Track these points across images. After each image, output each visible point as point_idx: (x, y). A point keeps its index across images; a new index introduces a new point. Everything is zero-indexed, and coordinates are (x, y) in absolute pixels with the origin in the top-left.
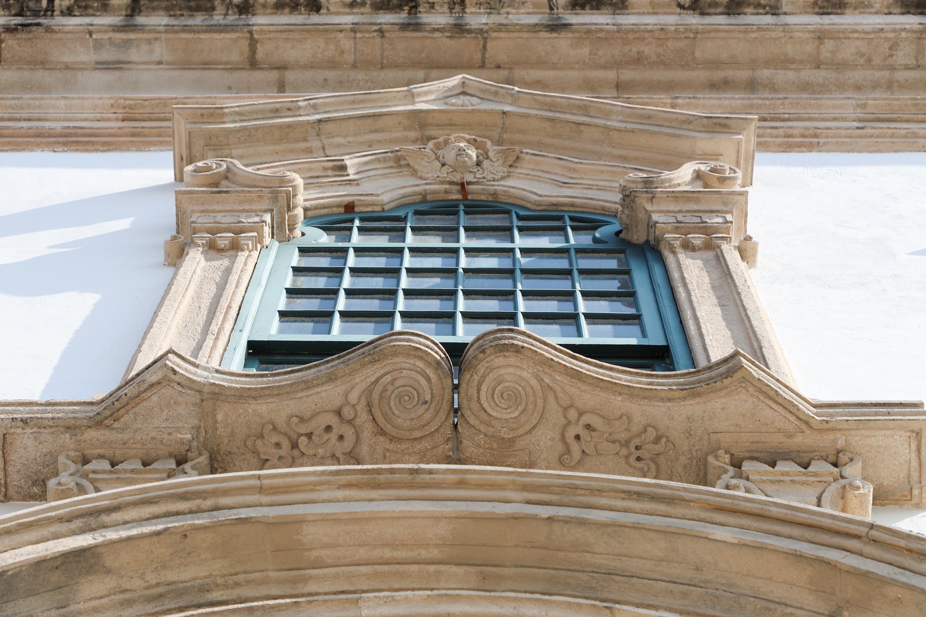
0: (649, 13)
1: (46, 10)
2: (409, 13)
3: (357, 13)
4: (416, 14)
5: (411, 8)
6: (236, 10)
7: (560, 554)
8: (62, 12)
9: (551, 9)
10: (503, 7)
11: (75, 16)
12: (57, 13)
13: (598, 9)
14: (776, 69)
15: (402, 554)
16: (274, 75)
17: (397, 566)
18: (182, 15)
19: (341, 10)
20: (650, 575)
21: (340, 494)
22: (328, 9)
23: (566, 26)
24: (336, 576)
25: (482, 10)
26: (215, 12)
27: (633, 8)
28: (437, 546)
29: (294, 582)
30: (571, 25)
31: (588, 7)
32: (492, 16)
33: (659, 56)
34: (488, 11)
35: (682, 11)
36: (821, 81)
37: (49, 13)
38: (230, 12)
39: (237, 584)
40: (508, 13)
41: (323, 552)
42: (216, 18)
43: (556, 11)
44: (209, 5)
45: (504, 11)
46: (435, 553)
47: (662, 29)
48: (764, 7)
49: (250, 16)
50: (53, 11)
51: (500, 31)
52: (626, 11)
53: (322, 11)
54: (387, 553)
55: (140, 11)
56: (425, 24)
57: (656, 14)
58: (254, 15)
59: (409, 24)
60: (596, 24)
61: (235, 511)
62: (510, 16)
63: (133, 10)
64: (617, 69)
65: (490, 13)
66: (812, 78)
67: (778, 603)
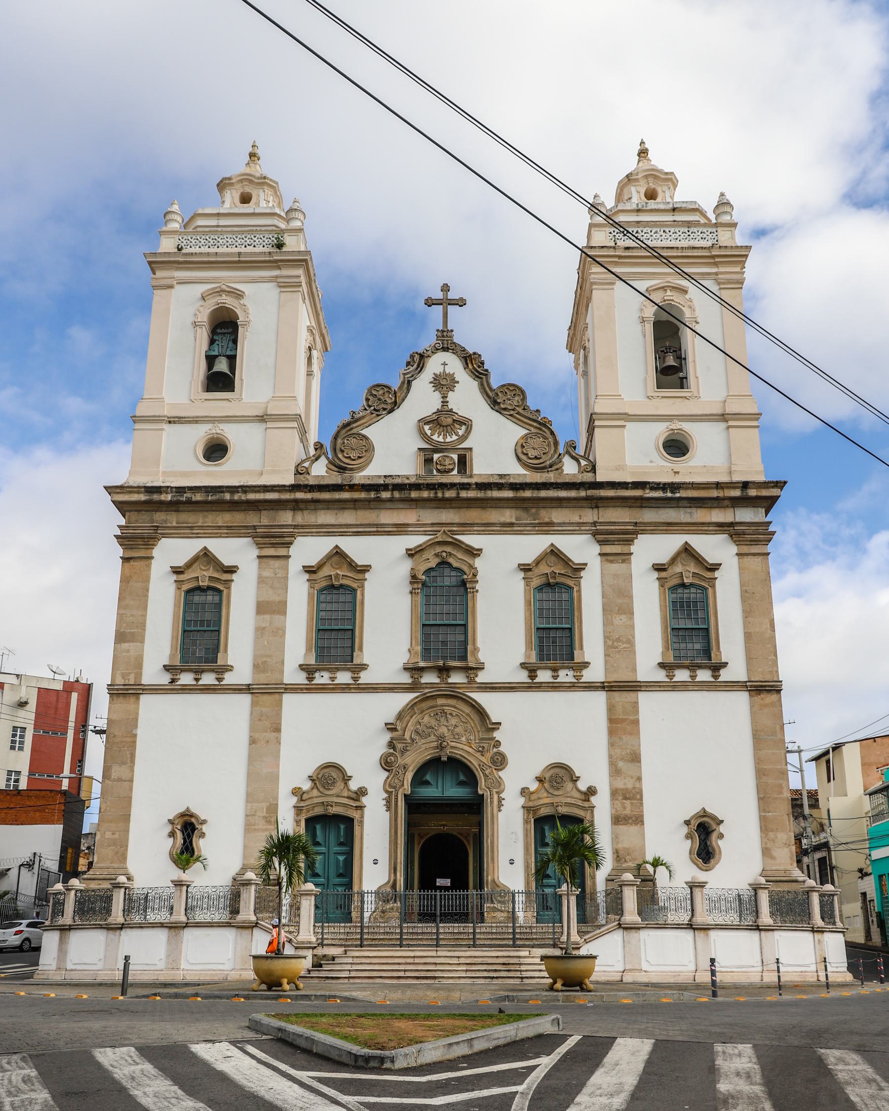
16: (415, 503)
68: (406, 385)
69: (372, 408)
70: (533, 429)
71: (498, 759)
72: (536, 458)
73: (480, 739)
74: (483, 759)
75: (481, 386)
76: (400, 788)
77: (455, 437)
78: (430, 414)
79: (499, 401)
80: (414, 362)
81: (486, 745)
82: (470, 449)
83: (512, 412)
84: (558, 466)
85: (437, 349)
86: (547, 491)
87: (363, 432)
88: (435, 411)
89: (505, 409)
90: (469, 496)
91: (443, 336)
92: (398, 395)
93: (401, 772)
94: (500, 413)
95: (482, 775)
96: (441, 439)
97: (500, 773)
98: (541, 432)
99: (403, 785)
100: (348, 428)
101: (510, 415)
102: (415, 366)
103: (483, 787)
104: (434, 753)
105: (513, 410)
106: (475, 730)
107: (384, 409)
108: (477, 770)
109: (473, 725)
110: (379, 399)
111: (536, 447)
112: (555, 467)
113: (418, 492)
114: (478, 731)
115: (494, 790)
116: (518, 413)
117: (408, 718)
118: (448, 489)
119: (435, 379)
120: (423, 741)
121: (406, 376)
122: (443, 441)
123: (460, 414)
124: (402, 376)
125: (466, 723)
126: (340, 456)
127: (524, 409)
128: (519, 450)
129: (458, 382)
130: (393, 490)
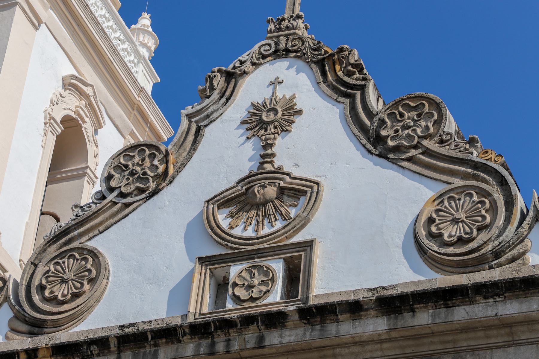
0: (294, 328)
1: (91, 355)
2: (212, 339)
3: (194, 341)
4: (214, 339)
5: (212, 336)
6: (153, 346)
8: (96, 355)
9: (260, 330)
10: (243, 332)
11: (101, 356)
12: (95, 356)
13: (276, 328)
14: (341, 348)
18: (136, 351)
19: (188, 341)
22: (184, 341)
23: (264, 347)
25: (236, 334)
26: (147, 348)
27: (288, 326)
30: (266, 346)
31: (272, 328)
32: (240, 337)
33: (300, 348)
34: (238, 334)
35: (305, 325)
36: (357, 351)
37: (92, 356)
38: (151, 347)
40: (245, 334)
42: (148, 350)
43: (261, 331)
44: (143, 346)
45: (244, 333)
47: (297, 344)
48: (333, 319)
49: (158, 348)
50: (93, 355)
51: (242, 351)
52: (286, 328)
53: (182, 342)
55: (122, 351)
56: (216, 353)
57: (297, 327)
58: (159, 347)
59: (211, 353)
60: (274, 345)
62: (246, 335)
63: (119, 351)
64: (287, 354)
65: (239, 335)
66: (354, 351)
68: (191, 137)
69: (115, 193)
70: (458, 182)
72: (461, 241)
75: (353, 108)
77: (278, 225)
78: (233, 184)
79: (383, 133)
80: (212, 88)
82: (309, 245)
83: (413, 152)
84: (515, 252)
85: (264, 57)
86: (468, 308)
87: (91, 244)
88: (247, 173)
89: (397, 149)
90: (285, 340)
91: (280, 29)
92: (171, 157)
94: (387, 158)
96: (250, 233)
98: (475, 183)
100: (64, 240)
101: (410, 160)
102: (216, 95)
105: (415, 147)
107: (141, 191)
110: (132, 174)
111: (463, 216)
112: (509, 255)
113: (175, 346)
116: (427, 152)
118: (240, 332)
119: (252, 115)
121: (193, 120)
122: (253, 235)
123: (295, 174)
124: (185, 122)
126: (36, 298)
127: (442, 142)
128: (422, 233)
129: (300, 112)
130: (119, 351)
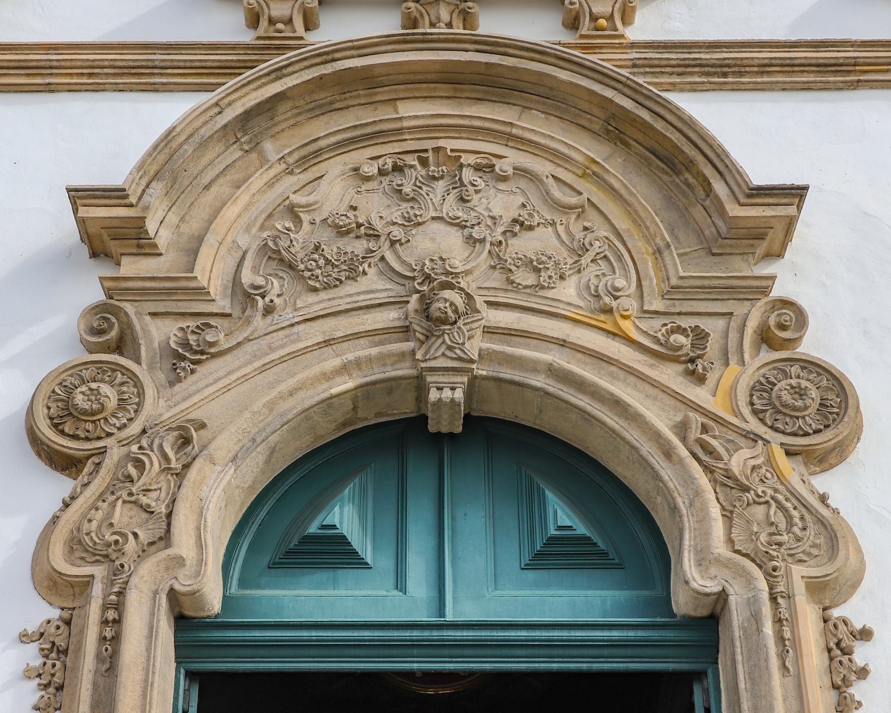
7: (490, 78)
15: (419, 77)
17: (417, 85)
20: (528, 91)
21: (389, 47)
24: (390, 91)
28: (434, 73)
29: (371, 95)
39: (346, 99)
41: (383, 78)
46: (433, 77)
54: (412, 77)
61: (342, 62)
67: (584, 111)
71: (801, 393)
73: (672, 292)
74: (699, 394)
76: (143, 554)
81: (713, 327)
93: (154, 464)
95: (703, 480)
97: (822, 482)
99: (166, 538)
103: (719, 546)
104: (382, 359)
106: (639, 246)
108: (668, 453)
109: (623, 224)
114: (658, 252)
115: (798, 571)
117: (220, 189)
120: (313, 303)
125: (580, 211)
